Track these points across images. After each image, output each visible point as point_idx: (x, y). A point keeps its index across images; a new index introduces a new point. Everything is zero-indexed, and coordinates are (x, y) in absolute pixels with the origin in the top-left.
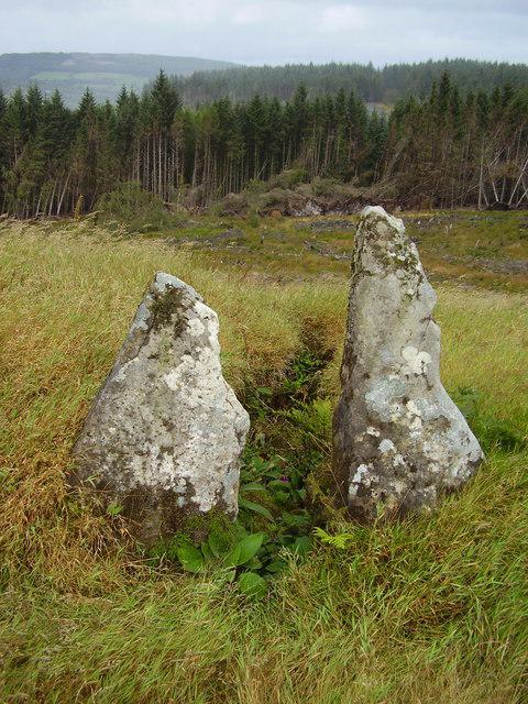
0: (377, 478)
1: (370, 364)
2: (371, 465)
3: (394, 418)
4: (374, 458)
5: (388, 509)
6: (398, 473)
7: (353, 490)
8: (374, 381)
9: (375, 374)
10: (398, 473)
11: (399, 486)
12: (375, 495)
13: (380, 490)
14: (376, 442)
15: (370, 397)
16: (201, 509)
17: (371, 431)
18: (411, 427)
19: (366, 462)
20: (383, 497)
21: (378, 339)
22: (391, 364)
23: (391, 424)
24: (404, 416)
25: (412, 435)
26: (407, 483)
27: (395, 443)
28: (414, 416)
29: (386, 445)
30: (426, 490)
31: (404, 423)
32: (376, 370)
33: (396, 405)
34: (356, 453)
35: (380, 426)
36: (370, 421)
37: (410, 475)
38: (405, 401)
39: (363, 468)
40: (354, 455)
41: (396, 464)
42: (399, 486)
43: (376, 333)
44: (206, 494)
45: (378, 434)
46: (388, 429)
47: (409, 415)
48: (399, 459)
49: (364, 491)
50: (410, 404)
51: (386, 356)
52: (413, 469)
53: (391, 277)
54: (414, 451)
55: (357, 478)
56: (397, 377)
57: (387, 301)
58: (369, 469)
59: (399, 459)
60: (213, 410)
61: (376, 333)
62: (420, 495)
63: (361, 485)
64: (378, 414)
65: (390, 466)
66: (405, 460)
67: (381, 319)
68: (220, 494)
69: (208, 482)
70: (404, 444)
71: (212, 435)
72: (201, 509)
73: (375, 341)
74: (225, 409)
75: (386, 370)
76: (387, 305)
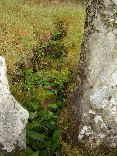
0: (92, 133)
1: (94, 82)
2: (90, 127)
3: (103, 107)
4: (91, 124)
5: (96, 146)
6: (102, 131)
7: (80, 137)
8: (95, 89)
9: (96, 87)
10: (102, 131)
11: (102, 136)
12: (91, 140)
13: (93, 137)
14: (93, 116)
15: (92, 98)
16: (8, 151)
17: (91, 112)
18: (111, 110)
19: (87, 125)
20: (95, 140)
21: (100, 69)
22: (105, 81)
23: (102, 109)
24: (108, 105)
25: (111, 114)
26: (106, 135)
27: (102, 118)
28: (113, 105)
29: (98, 118)
30: (114, 137)
31: (108, 108)
32: (97, 85)
33: (105, 100)
34: (83, 121)
35: (97, 110)
36: (91, 108)
37: (108, 131)
38: (110, 98)
39: (85, 128)
40: (81, 122)
41: (102, 127)
42: (102, 136)
43: (99, 66)
44: (9, 146)
45: (94, 113)
46: (100, 111)
47: (111, 105)
48: (104, 125)
49: (85, 137)
50: (112, 100)
51: (103, 78)
52: (110, 129)
53: (111, 34)
54: (111, 121)
55: (83, 132)
56: (107, 87)
57: (107, 48)
58: (89, 129)
59: (104, 125)
60: (7, 113)
61: (99, 66)
62: (112, 139)
63: (84, 135)
64: (95, 105)
65: (99, 128)
66: (106, 125)
67: (102, 58)
68: (17, 145)
69: (9, 142)
70: (107, 118)
71: (8, 124)
72: (8, 151)
73: (98, 71)
74: (14, 112)
75: (102, 84)
76: (107, 50)
